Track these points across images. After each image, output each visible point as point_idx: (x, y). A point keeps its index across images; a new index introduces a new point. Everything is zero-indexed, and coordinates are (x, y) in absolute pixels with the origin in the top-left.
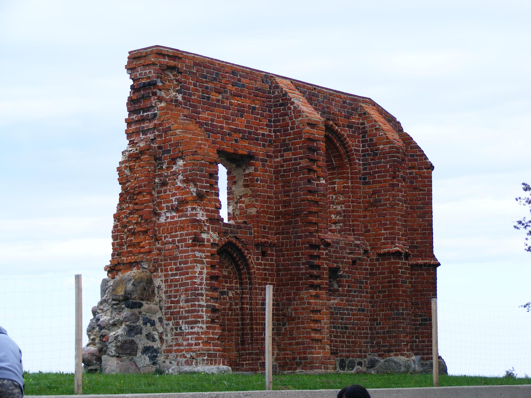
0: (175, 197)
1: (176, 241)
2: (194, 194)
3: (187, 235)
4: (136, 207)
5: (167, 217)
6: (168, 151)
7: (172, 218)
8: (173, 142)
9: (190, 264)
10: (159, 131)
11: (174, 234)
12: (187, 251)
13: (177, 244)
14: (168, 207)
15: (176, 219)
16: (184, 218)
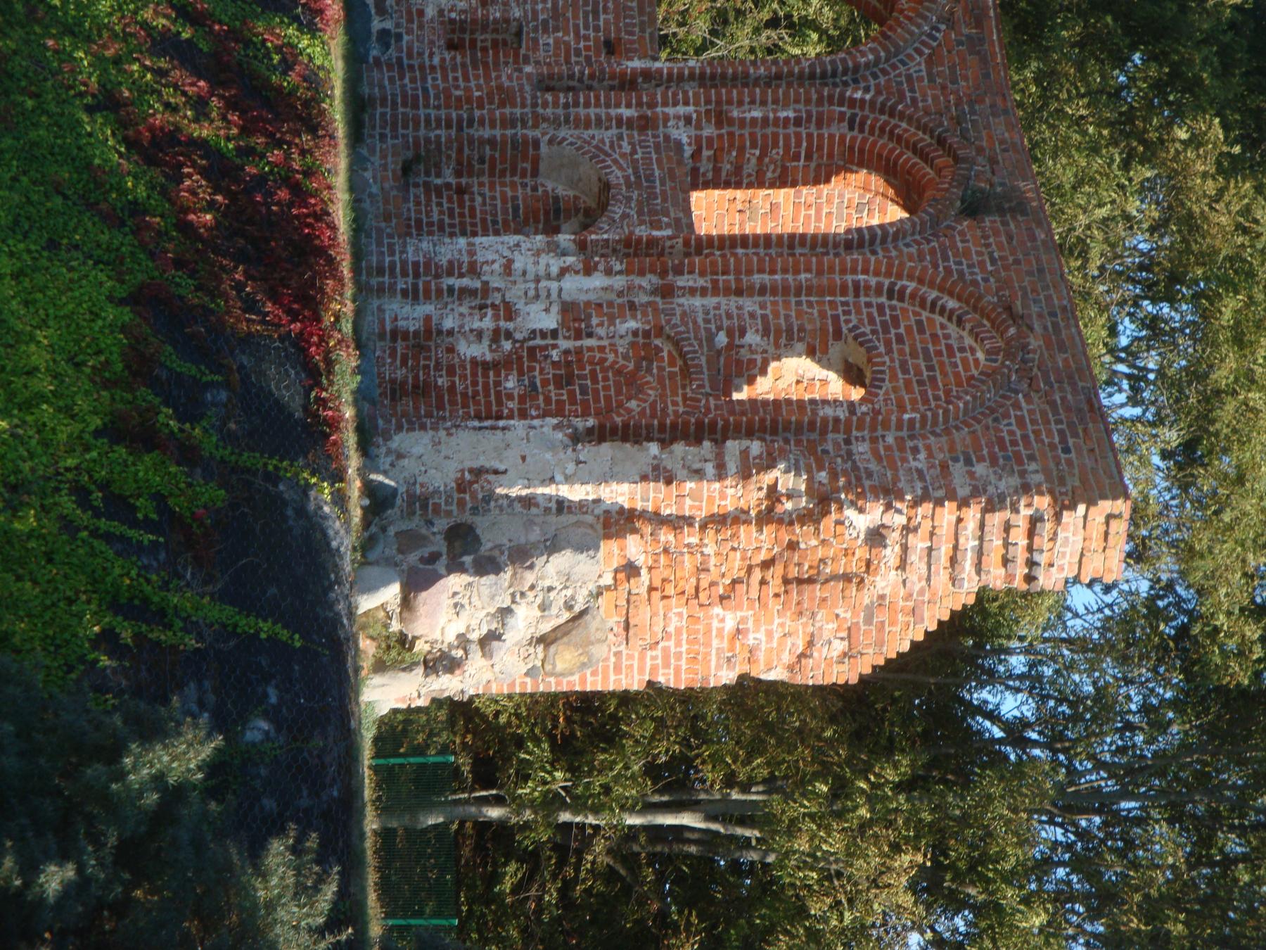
0: (764, 639)
1: (667, 644)
2: (763, 677)
3: (677, 670)
4: (757, 575)
5: (722, 620)
6: (868, 620)
7: (720, 631)
8: (887, 629)
9: (612, 677)
10: (921, 592)
11: (685, 636)
12: (641, 670)
13: (661, 644)
14: (743, 620)
15: (715, 643)
16: (713, 663)
